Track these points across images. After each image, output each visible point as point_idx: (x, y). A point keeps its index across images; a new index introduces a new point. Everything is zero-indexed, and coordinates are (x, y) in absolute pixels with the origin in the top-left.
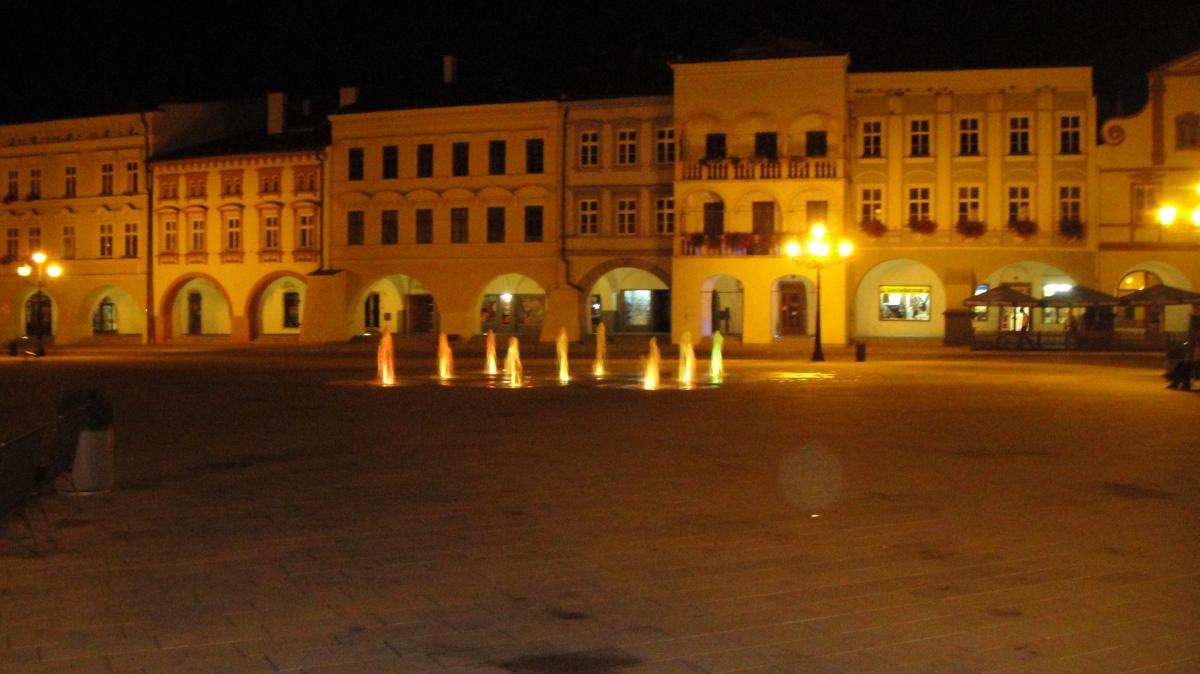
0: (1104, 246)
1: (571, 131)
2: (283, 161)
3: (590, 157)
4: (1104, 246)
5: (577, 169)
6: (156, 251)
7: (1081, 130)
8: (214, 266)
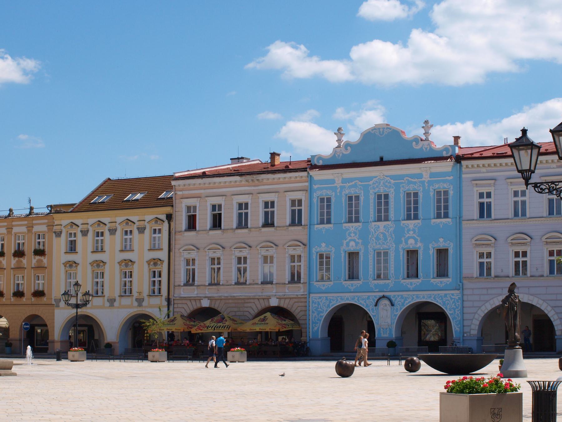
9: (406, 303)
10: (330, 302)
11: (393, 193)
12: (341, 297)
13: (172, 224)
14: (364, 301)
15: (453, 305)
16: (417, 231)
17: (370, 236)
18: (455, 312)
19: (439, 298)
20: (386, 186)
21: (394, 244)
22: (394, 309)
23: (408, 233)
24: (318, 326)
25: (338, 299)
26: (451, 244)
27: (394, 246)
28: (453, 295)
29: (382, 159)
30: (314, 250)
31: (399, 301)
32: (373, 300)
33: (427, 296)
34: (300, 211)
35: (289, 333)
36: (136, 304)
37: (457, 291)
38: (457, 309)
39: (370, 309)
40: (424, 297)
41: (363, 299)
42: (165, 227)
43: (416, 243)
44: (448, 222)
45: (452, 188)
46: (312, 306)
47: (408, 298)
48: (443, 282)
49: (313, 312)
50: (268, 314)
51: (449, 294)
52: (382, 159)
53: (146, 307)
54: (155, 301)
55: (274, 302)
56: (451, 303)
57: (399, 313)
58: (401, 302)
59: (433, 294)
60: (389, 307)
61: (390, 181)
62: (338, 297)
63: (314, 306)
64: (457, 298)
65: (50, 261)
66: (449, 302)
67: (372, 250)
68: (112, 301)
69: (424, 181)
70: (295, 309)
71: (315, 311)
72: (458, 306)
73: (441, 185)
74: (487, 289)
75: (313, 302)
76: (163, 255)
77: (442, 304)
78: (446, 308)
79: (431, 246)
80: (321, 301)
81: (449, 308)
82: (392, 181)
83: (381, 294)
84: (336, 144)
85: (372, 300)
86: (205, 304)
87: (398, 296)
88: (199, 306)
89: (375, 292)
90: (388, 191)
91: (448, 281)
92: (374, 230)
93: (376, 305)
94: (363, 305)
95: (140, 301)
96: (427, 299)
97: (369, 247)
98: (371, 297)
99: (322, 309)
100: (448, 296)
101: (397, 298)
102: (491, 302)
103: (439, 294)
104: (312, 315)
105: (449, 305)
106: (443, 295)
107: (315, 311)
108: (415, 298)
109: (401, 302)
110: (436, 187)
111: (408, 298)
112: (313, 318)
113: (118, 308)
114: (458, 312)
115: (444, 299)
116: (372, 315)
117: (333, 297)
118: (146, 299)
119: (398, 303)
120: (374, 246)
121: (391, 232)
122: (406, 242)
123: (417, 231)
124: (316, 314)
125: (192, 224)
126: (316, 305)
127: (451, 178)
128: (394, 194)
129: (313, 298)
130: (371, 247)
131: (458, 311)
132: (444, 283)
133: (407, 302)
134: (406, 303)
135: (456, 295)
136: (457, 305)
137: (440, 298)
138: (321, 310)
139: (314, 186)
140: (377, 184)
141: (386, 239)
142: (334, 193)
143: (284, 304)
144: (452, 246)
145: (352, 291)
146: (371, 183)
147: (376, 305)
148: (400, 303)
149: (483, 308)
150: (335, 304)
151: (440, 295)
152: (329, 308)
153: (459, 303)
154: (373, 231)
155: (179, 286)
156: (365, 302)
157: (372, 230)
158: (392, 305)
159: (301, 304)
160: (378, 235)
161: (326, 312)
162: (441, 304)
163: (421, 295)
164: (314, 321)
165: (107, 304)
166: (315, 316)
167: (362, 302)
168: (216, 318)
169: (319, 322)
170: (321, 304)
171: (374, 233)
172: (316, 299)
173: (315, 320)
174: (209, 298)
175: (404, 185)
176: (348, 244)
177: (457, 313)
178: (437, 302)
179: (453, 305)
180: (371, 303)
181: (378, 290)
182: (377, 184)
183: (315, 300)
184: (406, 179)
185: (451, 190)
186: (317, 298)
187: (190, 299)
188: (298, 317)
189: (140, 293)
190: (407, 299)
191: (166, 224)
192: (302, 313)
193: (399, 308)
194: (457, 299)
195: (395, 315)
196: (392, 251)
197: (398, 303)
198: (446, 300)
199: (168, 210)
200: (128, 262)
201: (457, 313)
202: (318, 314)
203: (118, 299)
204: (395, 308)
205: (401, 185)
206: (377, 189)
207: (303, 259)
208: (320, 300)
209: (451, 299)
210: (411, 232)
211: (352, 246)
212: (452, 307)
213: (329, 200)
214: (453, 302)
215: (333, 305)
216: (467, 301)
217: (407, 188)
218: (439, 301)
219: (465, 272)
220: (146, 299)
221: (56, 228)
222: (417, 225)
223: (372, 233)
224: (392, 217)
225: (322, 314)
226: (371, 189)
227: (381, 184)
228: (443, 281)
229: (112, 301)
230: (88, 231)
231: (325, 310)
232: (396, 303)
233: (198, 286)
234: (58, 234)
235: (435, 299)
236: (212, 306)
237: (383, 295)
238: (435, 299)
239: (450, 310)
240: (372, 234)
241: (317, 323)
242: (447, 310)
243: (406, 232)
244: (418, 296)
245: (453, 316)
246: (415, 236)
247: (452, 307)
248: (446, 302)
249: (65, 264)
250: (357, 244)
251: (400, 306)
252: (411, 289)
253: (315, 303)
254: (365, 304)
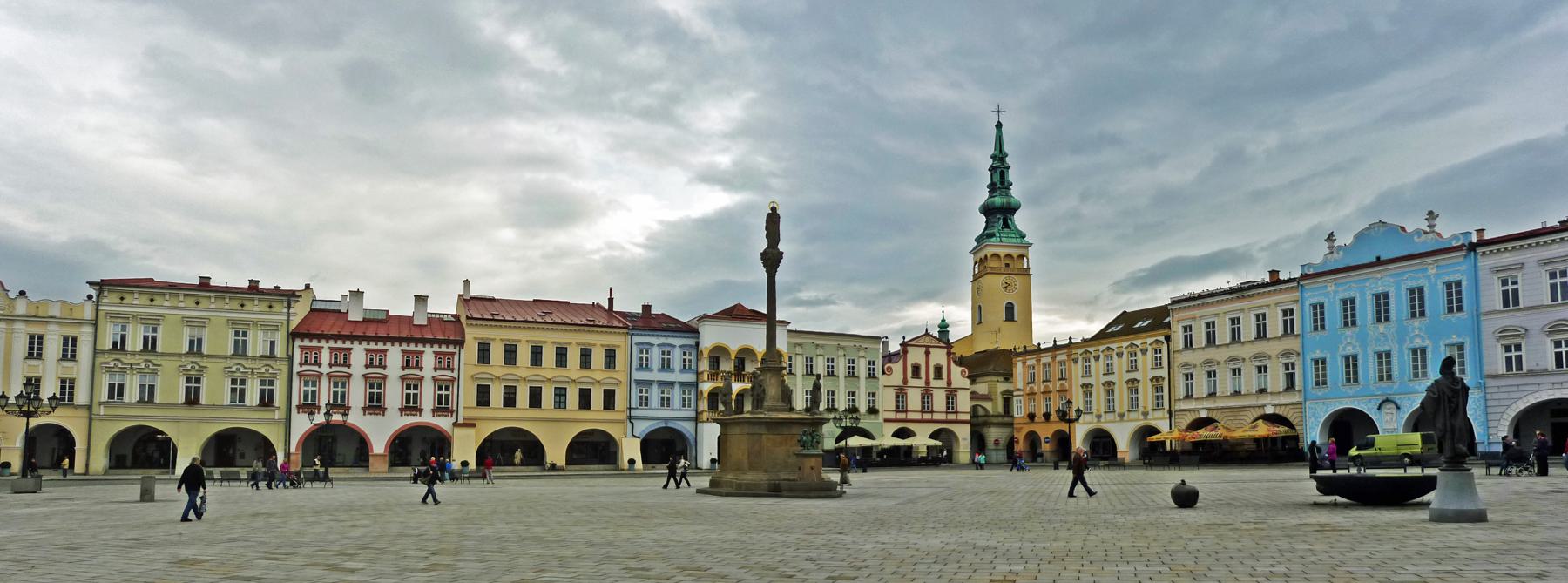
0: (887, 420)
1: (635, 348)
2: (424, 346)
3: (645, 365)
4: (887, 420)
5: (637, 370)
6: (295, 402)
7: (876, 367)
8: (356, 419)
13: (1171, 344)
30: (1308, 358)
34: (1292, 320)
35: (1285, 439)
36: (1142, 417)
42: (1164, 348)
49: (1310, 418)
50: (1260, 421)
53: (1151, 420)
54: (1159, 414)
55: (1269, 410)
57: (1406, 416)
60: (1394, 410)
64: (1478, 397)
65: (1071, 385)
68: (1122, 416)
70: (1291, 415)
74: (1518, 385)
76: (1163, 373)
83: (1385, 397)
86: (1204, 414)
88: (1198, 416)
95: (1145, 414)
102: (1525, 400)
113: (1128, 421)
118: (1150, 412)
122: (1412, 343)
124: (1313, 419)
125: (1188, 343)
141: (1387, 340)
143: (1280, 411)
147: (1379, 408)
149: (1514, 407)
153: (1482, 402)
155: (1180, 400)
158: (1398, 408)
159: (1297, 410)
165: (1118, 419)
168: (1209, 427)
174: (1207, 409)
176: (1344, 349)
181: (1379, 393)
187: (1189, 410)
188: (1294, 423)
189: (1145, 408)
191: (1165, 345)
192: (1299, 419)
199: (1166, 331)
200: (1134, 381)
203: (1126, 414)
207: (1296, 367)
213: (1322, 306)
219: (1487, 370)
220: (1150, 412)
221: (1073, 357)
229: (1122, 416)
230: (1099, 356)
232: (1401, 405)
233: (1197, 399)
234: (1076, 361)
236: (1210, 416)
249: (1082, 386)
250: (1354, 347)
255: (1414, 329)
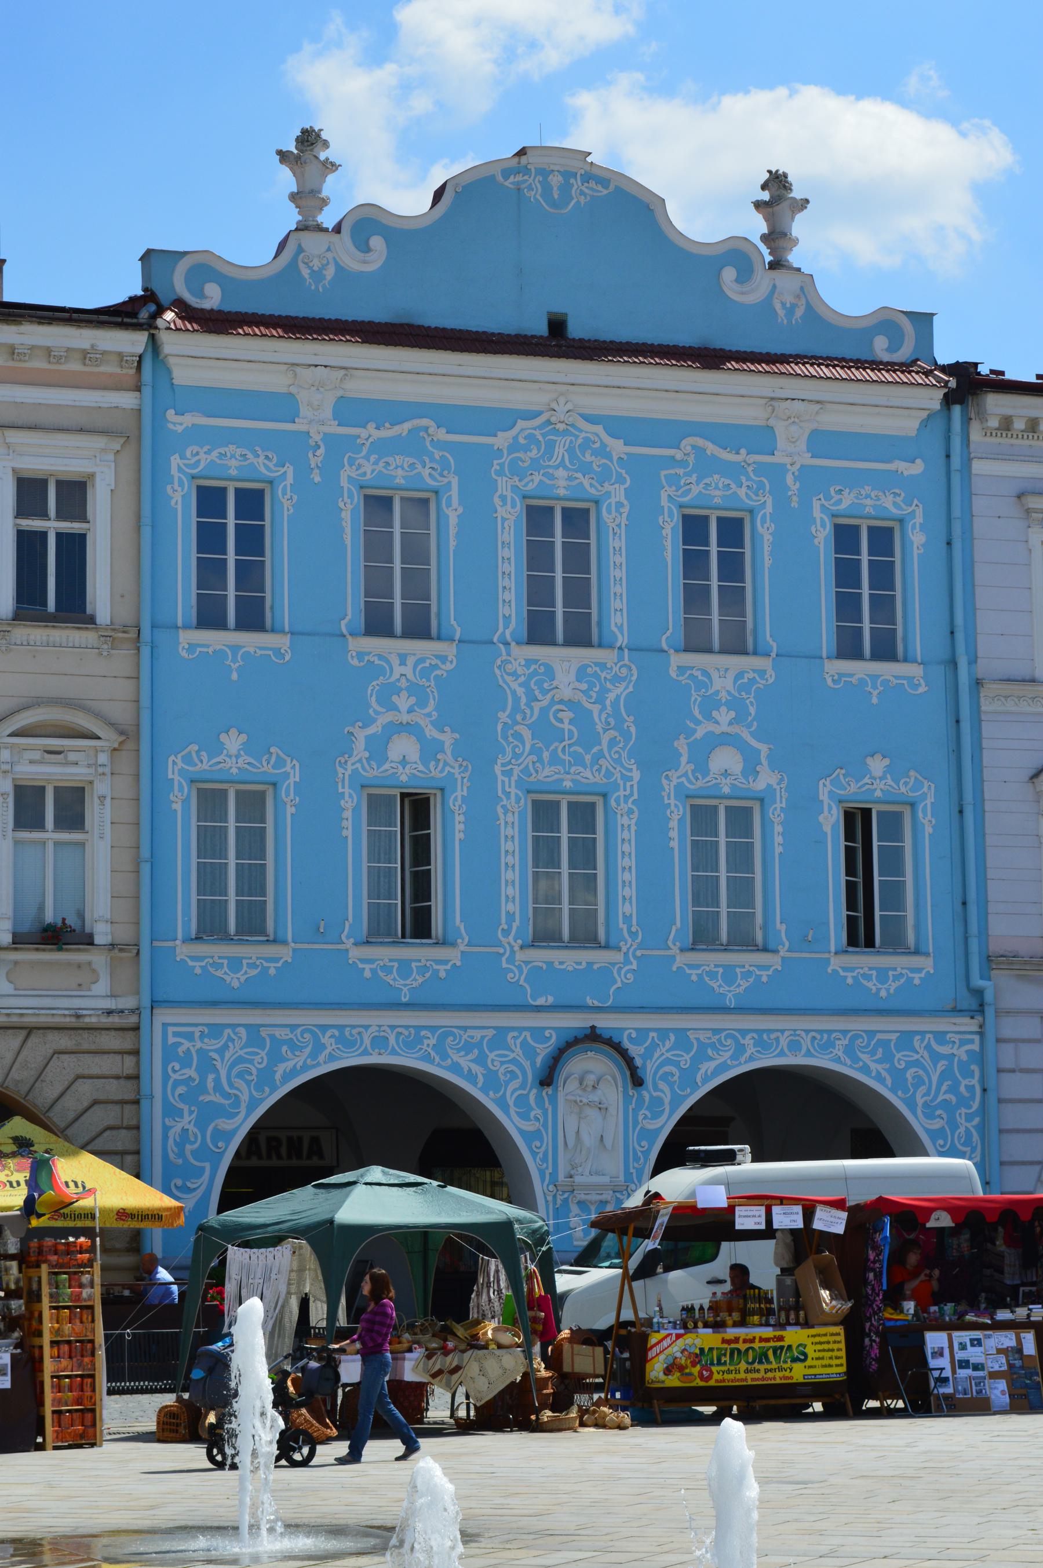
9: (702, 1071)
10: (275, 1057)
11: (620, 505)
12: (341, 1028)
14: (471, 1057)
15: (944, 1088)
16: (752, 710)
17: (503, 716)
18: (953, 1125)
19: (873, 1053)
20: (586, 469)
21: (634, 767)
22: (641, 1101)
23: (709, 717)
24: (199, 1194)
25: (326, 1040)
26: (925, 789)
27: (636, 775)
28: (940, 1037)
29: (557, 326)
30: (174, 768)
31: (668, 1062)
32: (529, 1052)
33: (814, 1038)
37: (967, 1020)
38: (963, 1111)
39: (511, 1102)
40: (794, 1046)
41: (468, 1048)
43: (751, 769)
44: (910, 679)
45: (919, 519)
46: (166, 1077)
47: (713, 1046)
48: (891, 973)
49: (171, 1111)
51: (923, 1033)
52: (557, 326)
56: (935, 1079)
58: (677, 1064)
59: (845, 1032)
61: (604, 445)
62: (324, 1028)
63: (174, 1076)
64: (962, 1053)
66: (921, 1072)
67: (513, 790)
69: (781, 468)
71: (181, 1105)
72: (966, 1094)
73: (868, 496)
75: (170, 1053)
77: (889, 1081)
78: (912, 1105)
79: (826, 790)
80: (221, 1051)
81: (926, 1105)
82: (617, 447)
84: (291, 217)
85: (518, 1053)
87: (663, 1033)
89: (538, 1009)
90: (593, 491)
91: (912, 970)
92: (525, 685)
93: (547, 1079)
94: (471, 1077)
96: (814, 1056)
97: (498, 769)
98: (515, 1034)
99: (228, 1096)
100: (916, 1044)
101: (654, 1046)
103: (871, 1034)
104: (166, 1129)
105: (923, 1089)
106: (894, 1037)
107: (181, 1105)
108: (750, 1050)
109: (677, 1064)
110: (840, 501)
111: (713, 1046)
112: (171, 1142)
114: (968, 1125)
115: (900, 1058)
116: (521, 1132)
117: (293, 1027)
119: (661, 1072)
120: (526, 771)
121: (615, 703)
122: (701, 767)
123: (752, 710)
124: (187, 1121)
126: (191, 1072)
127: (917, 468)
128: (626, 510)
129: (171, 1030)
130: (508, 773)
131: (969, 1118)
132: (896, 978)
133: (709, 1066)
134: (702, 1071)
135: (957, 1041)
136: (962, 1089)
137: (879, 1055)
138: (218, 1099)
139: (170, 414)
140: (534, 453)
142: (289, 470)
144: (930, 800)
145: (404, 1000)
146: (502, 440)
147: (547, 1079)
148: (674, 1070)
150: (305, 1068)
151: (879, 1036)
152: (267, 1090)
154: (520, 691)
156: (481, 1060)
157: (514, 686)
160: (544, 711)
161: (250, 1110)
162: (879, 1078)
163: (782, 1031)
164: (180, 1161)
166: (185, 1131)
167: (465, 1062)
169: (207, 1166)
170: (218, 1064)
171: (524, 700)
172: (190, 1037)
173: (181, 1154)
175: (681, 471)
176: (378, 749)
177: (962, 1130)
178: (865, 1069)
179: (944, 1088)
180: (512, 1067)
182: (534, 453)
183: (187, 1044)
184: (694, 447)
185: (914, 527)
186: (197, 1035)
190: (710, 1052)
193: (667, 1101)
194: (964, 1057)
195: (649, 1135)
196: (626, 802)
197: (661, 1072)
198: (910, 1064)
201: (962, 1130)
202: (201, 1123)
204: (645, 1093)
205: (663, 473)
206: (537, 478)
208: (212, 1045)
209: (936, 1057)
210: (724, 717)
211: (404, 762)
212: (940, 1098)
214: (944, 1076)
215: (293, 1073)
216: (1013, 1071)
217: (696, 490)
218: (873, 1066)
222: (752, 681)
223: (516, 699)
224: (620, 628)
225: (225, 1124)
226: (500, 473)
227: (560, 451)
228: (895, 969)
231: (245, 1097)
232: (649, 1070)
235: (855, 1059)
237: (593, 1028)
238: (855, 1059)
239: (929, 1116)
240: (516, 708)
241: (199, 1172)
242: (915, 1114)
243: (696, 712)
244: (765, 1036)
245: (941, 1146)
246: (746, 736)
247: (940, 1098)
248: (909, 1074)
250: (430, 751)
251: (671, 1085)
252: (731, 1001)
253: (186, 1062)
254: (476, 1068)
255: (710, 705)
